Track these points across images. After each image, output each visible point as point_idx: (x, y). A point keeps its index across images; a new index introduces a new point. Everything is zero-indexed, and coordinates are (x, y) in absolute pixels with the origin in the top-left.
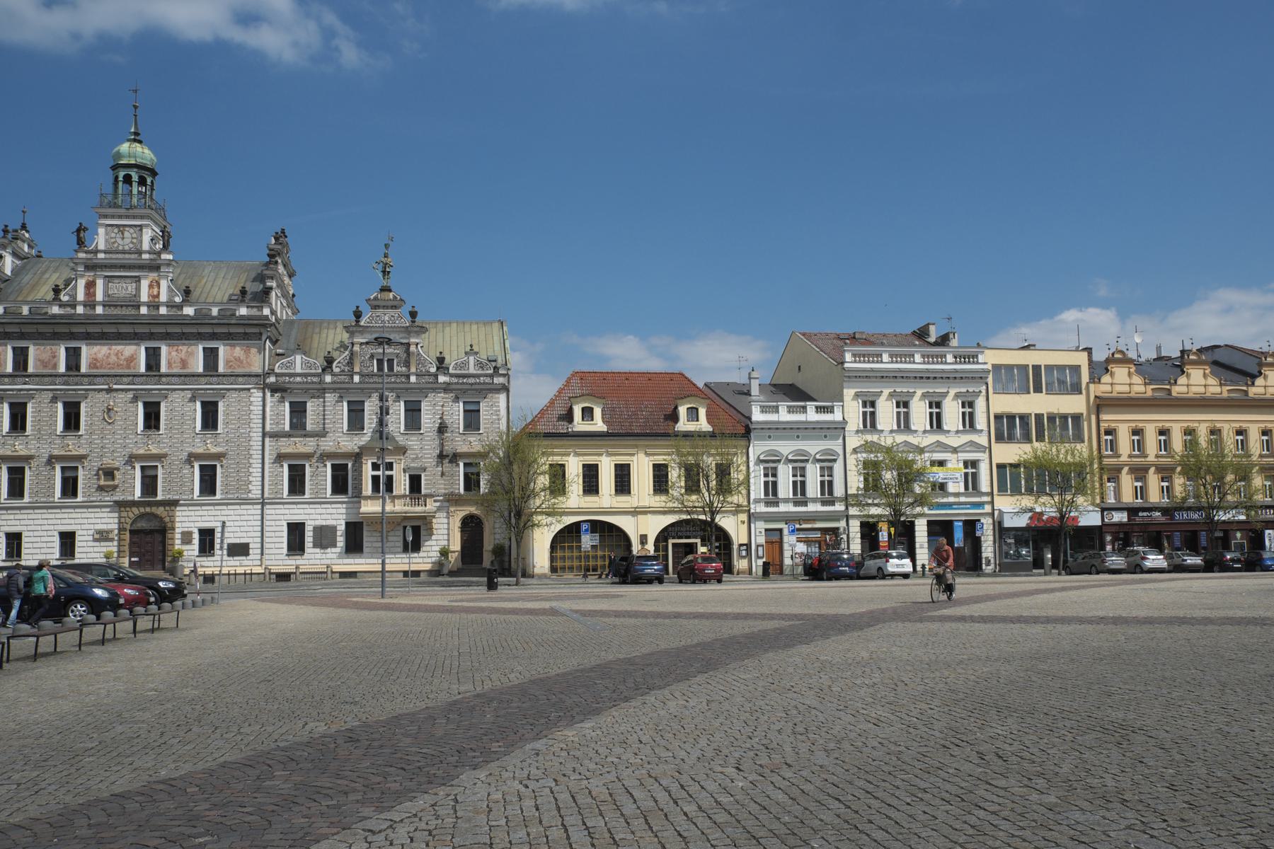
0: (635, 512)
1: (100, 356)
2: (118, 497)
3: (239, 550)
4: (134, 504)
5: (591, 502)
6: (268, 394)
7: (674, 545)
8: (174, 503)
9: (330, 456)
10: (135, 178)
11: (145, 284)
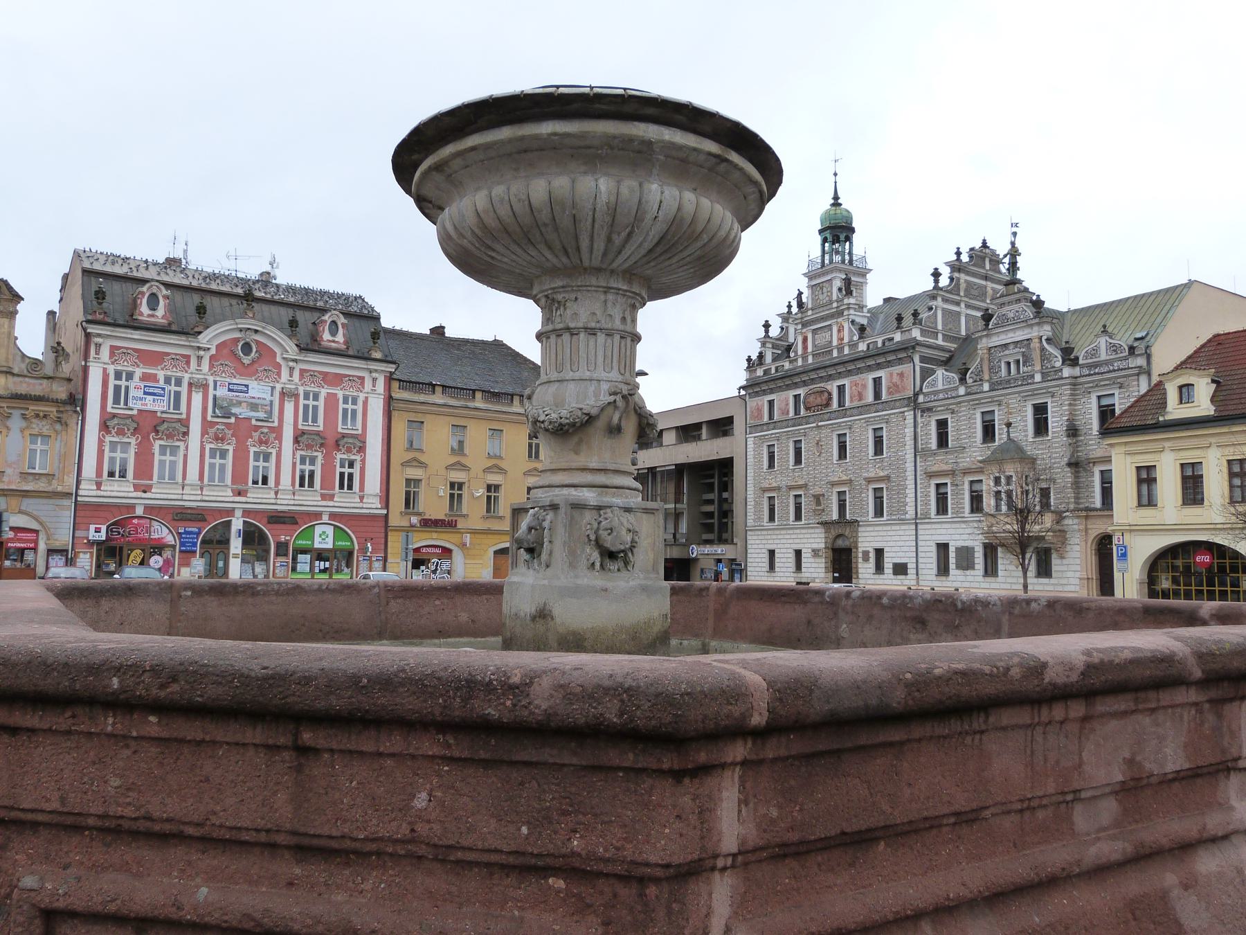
2: (825, 518)
3: (900, 569)
4: (833, 523)
5: (1193, 514)
6: (919, 415)
9: (966, 472)
10: (830, 238)
11: (835, 329)
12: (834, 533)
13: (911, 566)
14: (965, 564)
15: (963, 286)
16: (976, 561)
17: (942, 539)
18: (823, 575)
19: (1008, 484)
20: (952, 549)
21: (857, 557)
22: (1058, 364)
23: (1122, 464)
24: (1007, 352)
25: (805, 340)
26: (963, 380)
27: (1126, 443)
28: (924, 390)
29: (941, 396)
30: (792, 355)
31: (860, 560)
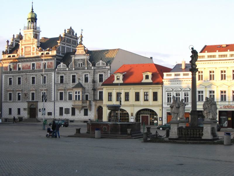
0: (131, 106)
1: (24, 66)
3: (50, 114)
4: (30, 102)
6: (56, 73)
7: (142, 116)
8: (37, 102)
12: (30, 104)
13: (53, 113)
14: (67, 113)
15: (66, 39)
16: (70, 112)
17: (61, 106)
18: (27, 115)
19: (79, 93)
20: (64, 109)
21: (37, 111)
22: (91, 66)
23: (105, 91)
24: (79, 61)
25: (22, 49)
26: (68, 66)
27: (106, 87)
28: (57, 68)
29: (62, 70)
30: (18, 53)
31: (38, 111)
